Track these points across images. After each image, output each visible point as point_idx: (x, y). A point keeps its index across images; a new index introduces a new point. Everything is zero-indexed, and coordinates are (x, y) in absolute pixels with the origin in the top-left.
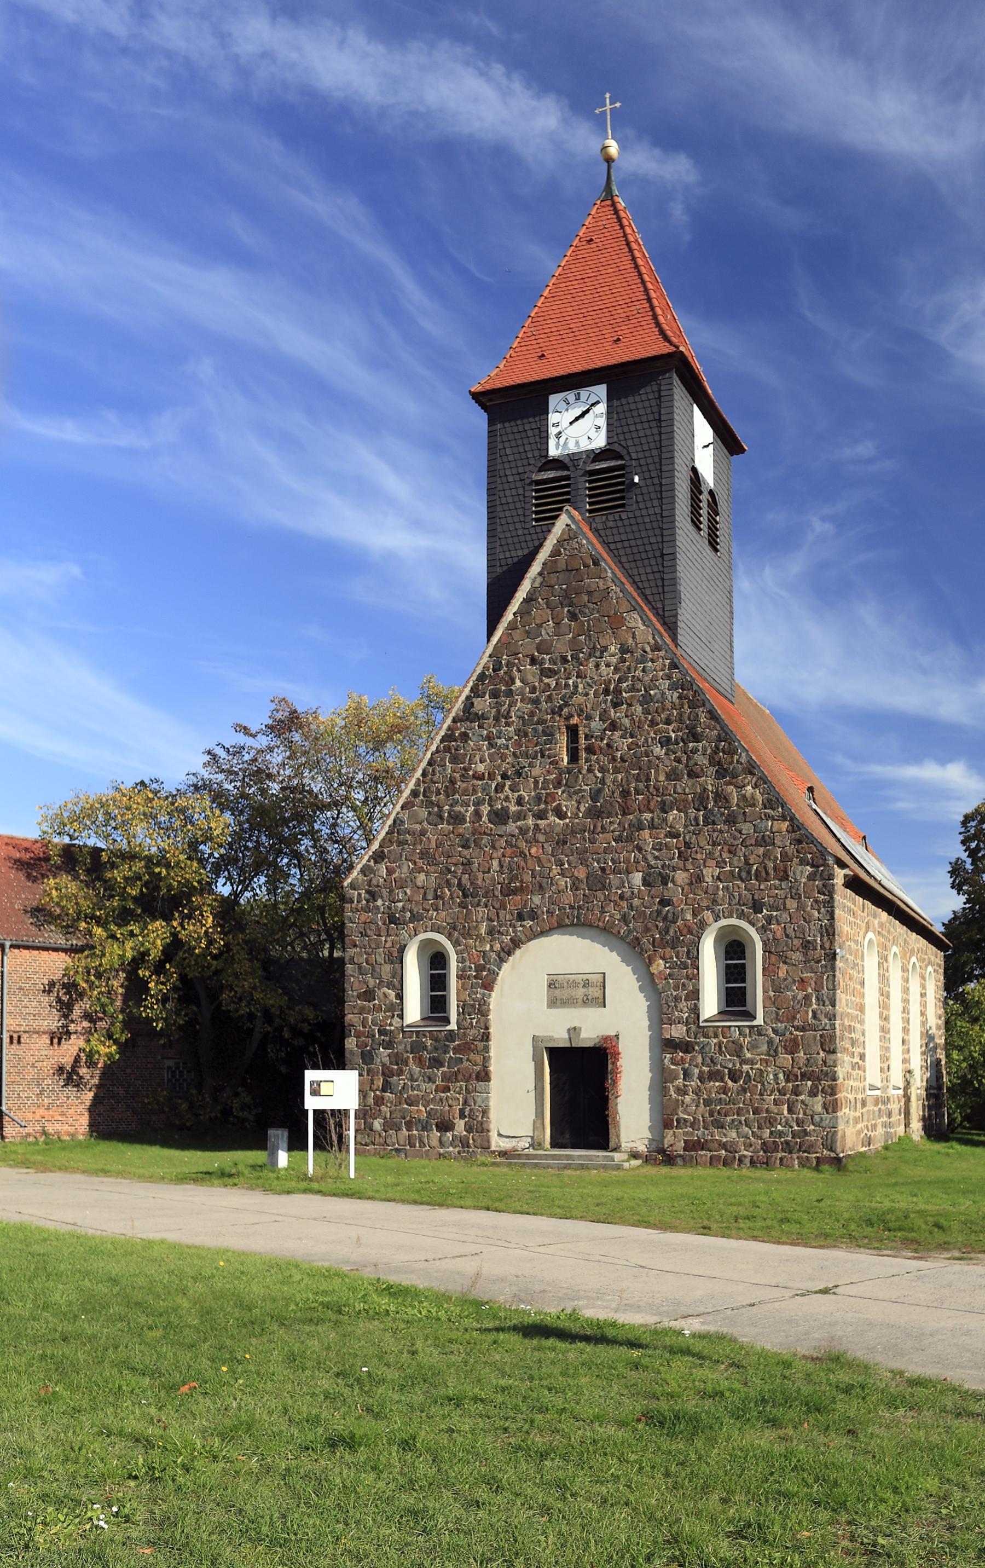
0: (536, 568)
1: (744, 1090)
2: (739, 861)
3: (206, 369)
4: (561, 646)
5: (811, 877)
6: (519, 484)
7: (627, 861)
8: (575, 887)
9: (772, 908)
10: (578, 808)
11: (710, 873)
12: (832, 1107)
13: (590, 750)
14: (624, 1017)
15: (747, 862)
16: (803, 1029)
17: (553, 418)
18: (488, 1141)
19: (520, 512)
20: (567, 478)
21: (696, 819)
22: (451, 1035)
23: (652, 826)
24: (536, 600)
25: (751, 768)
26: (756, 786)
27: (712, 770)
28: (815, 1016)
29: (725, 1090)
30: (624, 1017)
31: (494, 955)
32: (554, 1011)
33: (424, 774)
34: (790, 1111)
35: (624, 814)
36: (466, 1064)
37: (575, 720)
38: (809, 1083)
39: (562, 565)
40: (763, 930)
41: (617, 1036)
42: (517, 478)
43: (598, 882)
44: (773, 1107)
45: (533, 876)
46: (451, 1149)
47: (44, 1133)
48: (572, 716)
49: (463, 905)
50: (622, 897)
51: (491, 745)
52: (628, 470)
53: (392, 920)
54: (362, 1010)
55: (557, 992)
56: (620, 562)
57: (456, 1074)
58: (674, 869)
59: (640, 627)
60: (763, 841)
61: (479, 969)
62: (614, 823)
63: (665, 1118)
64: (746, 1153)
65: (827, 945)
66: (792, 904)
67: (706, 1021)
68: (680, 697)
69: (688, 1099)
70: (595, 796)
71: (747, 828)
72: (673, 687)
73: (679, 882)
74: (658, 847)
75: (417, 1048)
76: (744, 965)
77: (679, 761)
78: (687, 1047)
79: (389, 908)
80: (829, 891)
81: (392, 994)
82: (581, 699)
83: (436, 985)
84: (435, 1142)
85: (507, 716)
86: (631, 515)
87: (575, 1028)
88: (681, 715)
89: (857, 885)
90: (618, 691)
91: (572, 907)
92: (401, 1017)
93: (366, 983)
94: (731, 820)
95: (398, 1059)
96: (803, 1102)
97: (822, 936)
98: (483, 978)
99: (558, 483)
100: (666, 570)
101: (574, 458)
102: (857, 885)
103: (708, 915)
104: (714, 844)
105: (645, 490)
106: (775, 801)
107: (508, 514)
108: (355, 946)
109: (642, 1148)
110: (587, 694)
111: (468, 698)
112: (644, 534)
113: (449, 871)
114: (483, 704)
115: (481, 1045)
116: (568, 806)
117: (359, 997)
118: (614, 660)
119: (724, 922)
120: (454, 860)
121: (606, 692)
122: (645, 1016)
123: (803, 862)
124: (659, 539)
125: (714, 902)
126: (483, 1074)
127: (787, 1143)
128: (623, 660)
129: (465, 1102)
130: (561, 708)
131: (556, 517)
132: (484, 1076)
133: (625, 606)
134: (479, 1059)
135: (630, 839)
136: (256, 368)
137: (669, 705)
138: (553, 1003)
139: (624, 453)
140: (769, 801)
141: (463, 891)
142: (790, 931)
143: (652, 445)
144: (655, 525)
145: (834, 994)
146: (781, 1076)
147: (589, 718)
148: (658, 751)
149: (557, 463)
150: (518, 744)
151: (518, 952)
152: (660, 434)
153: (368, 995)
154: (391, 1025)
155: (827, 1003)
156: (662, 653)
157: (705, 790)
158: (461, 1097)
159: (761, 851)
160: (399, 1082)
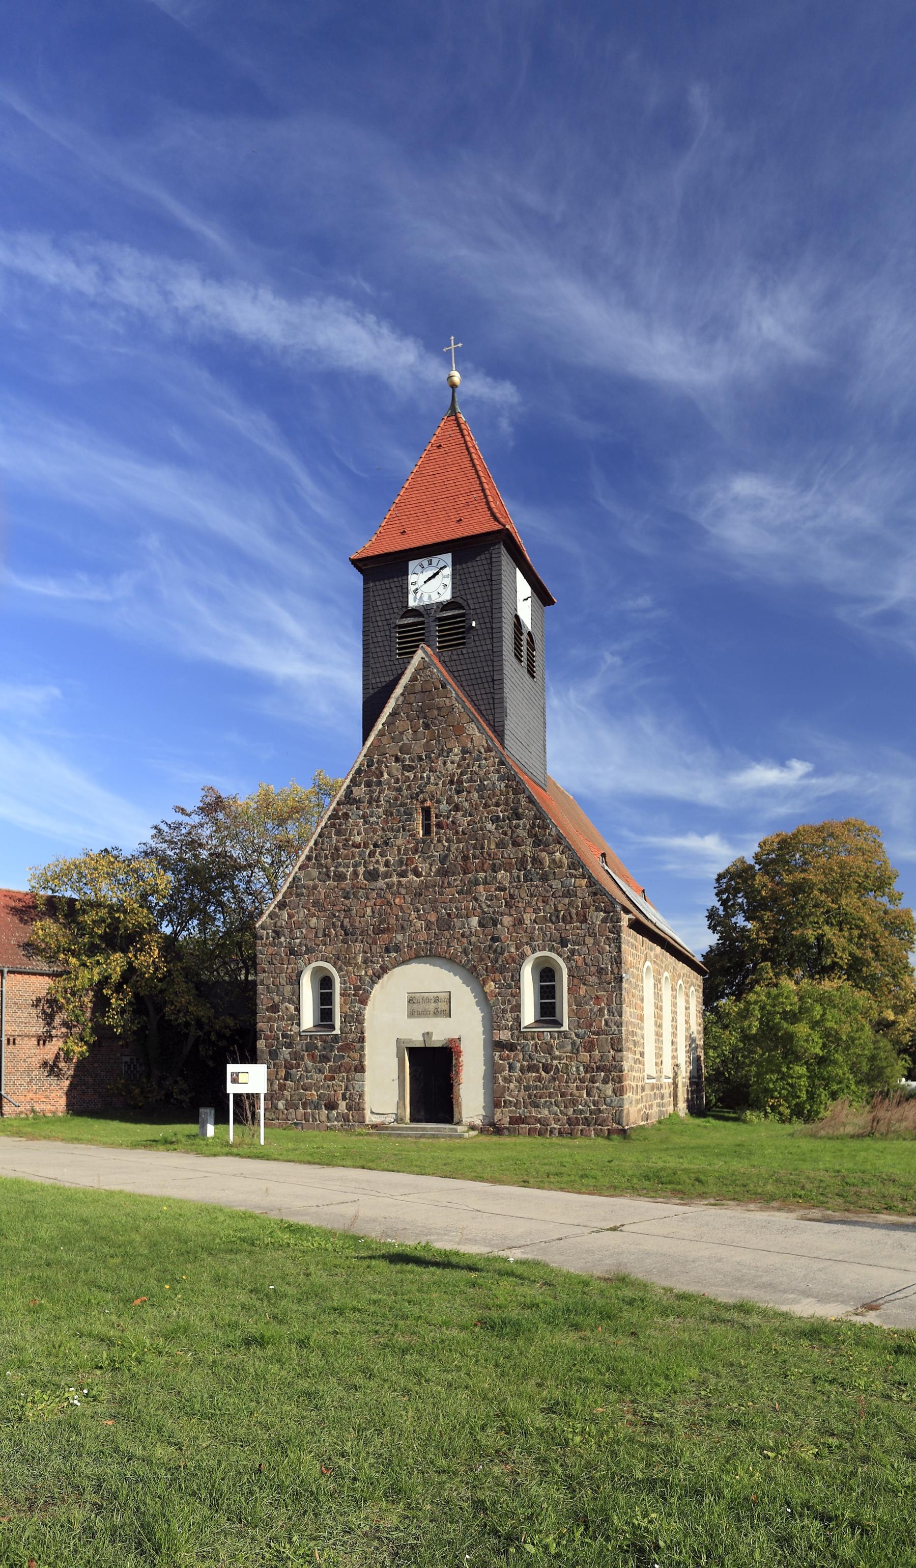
0: (399, 690)
1: (554, 1079)
2: (550, 908)
4: (418, 748)
5: (604, 921)
6: (386, 628)
7: (467, 908)
8: (428, 928)
9: (574, 943)
10: (430, 869)
11: (528, 917)
12: (619, 1092)
13: (439, 826)
14: (464, 1025)
15: (556, 910)
16: (598, 1034)
17: (412, 578)
18: (364, 1117)
19: (387, 648)
20: (422, 623)
21: (518, 877)
22: (336, 1038)
23: (486, 882)
24: (399, 714)
25: (559, 839)
26: (563, 853)
27: (531, 840)
28: (606, 1024)
29: (539, 1079)
30: (464, 1025)
31: (367, 979)
32: (413, 1020)
33: (316, 844)
34: (588, 1094)
35: (465, 873)
36: (347, 1059)
37: (428, 804)
38: (603, 1074)
39: (418, 688)
40: (568, 960)
41: (459, 1039)
42: (385, 623)
43: (445, 924)
44: (575, 1092)
45: (397, 920)
46: (336, 1123)
48: (426, 800)
49: (344, 942)
50: (463, 935)
51: (366, 822)
52: (467, 617)
53: (292, 952)
54: (270, 1019)
55: (415, 1005)
56: (462, 686)
57: (340, 1067)
58: (502, 914)
59: (477, 734)
60: (568, 894)
61: (357, 989)
62: (457, 880)
63: (495, 1100)
64: (555, 1126)
65: (616, 971)
66: (589, 941)
67: (525, 1028)
68: (506, 787)
69: (512, 1086)
70: (443, 859)
71: (556, 884)
72: (501, 779)
73: (506, 924)
74: (490, 898)
75: (310, 1047)
76: (554, 986)
77: (505, 834)
78: (511, 1047)
79: (290, 943)
80: (617, 931)
81: (292, 1007)
82: (433, 788)
83: (325, 999)
84: (324, 1118)
85: (378, 801)
86: (470, 650)
88: (507, 799)
89: (639, 926)
90: (460, 782)
91: (426, 943)
92: (299, 1024)
93: (272, 999)
94: (544, 878)
95: (297, 1056)
96: (598, 1088)
97: (612, 964)
98: (359, 995)
99: (415, 626)
100: (496, 692)
101: (428, 608)
102: (639, 926)
103: (527, 948)
104: (532, 896)
105: (480, 632)
106: (577, 864)
107: (378, 649)
108: (264, 972)
109: (478, 1122)
110: (437, 784)
111: (348, 787)
112: (479, 665)
113: (335, 916)
114: (360, 792)
115: (358, 1046)
116: (423, 867)
117: (267, 1010)
118: (457, 759)
119: (539, 954)
120: (338, 908)
121: (452, 782)
123: (598, 909)
124: (491, 669)
125: (532, 939)
127: (586, 1118)
128: (464, 759)
129: (347, 1088)
130: (417, 794)
131: (414, 652)
132: (360, 1069)
133: (465, 719)
134: (356, 1056)
135: (469, 892)
137: (498, 792)
138: (412, 1014)
139: (464, 604)
140: (573, 863)
141: (345, 931)
142: (588, 961)
143: (486, 599)
144: (488, 658)
145: (621, 1008)
146: (581, 1068)
147: (438, 802)
148: (490, 826)
149: (415, 612)
150: (386, 821)
151: (386, 976)
152: (491, 590)
153: (274, 1008)
154: (291, 1030)
155: (616, 1014)
156: (493, 754)
157: (525, 855)
158: (343, 1084)
159: (567, 901)
160: (297, 1073)
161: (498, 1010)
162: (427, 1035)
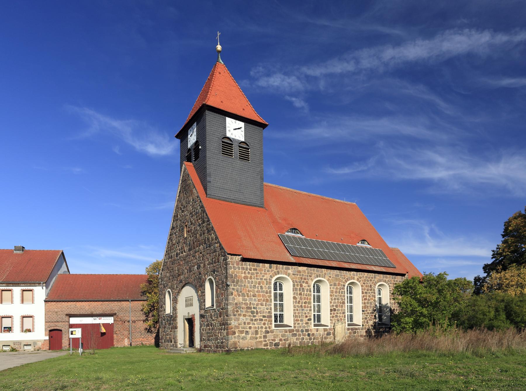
3: (381, 144)
40: (215, 279)
47: (142, 344)
94: (210, 246)
123: (222, 256)
136: (394, 140)
138: (187, 306)
148: (198, 228)
153: (162, 307)
161: (202, 301)
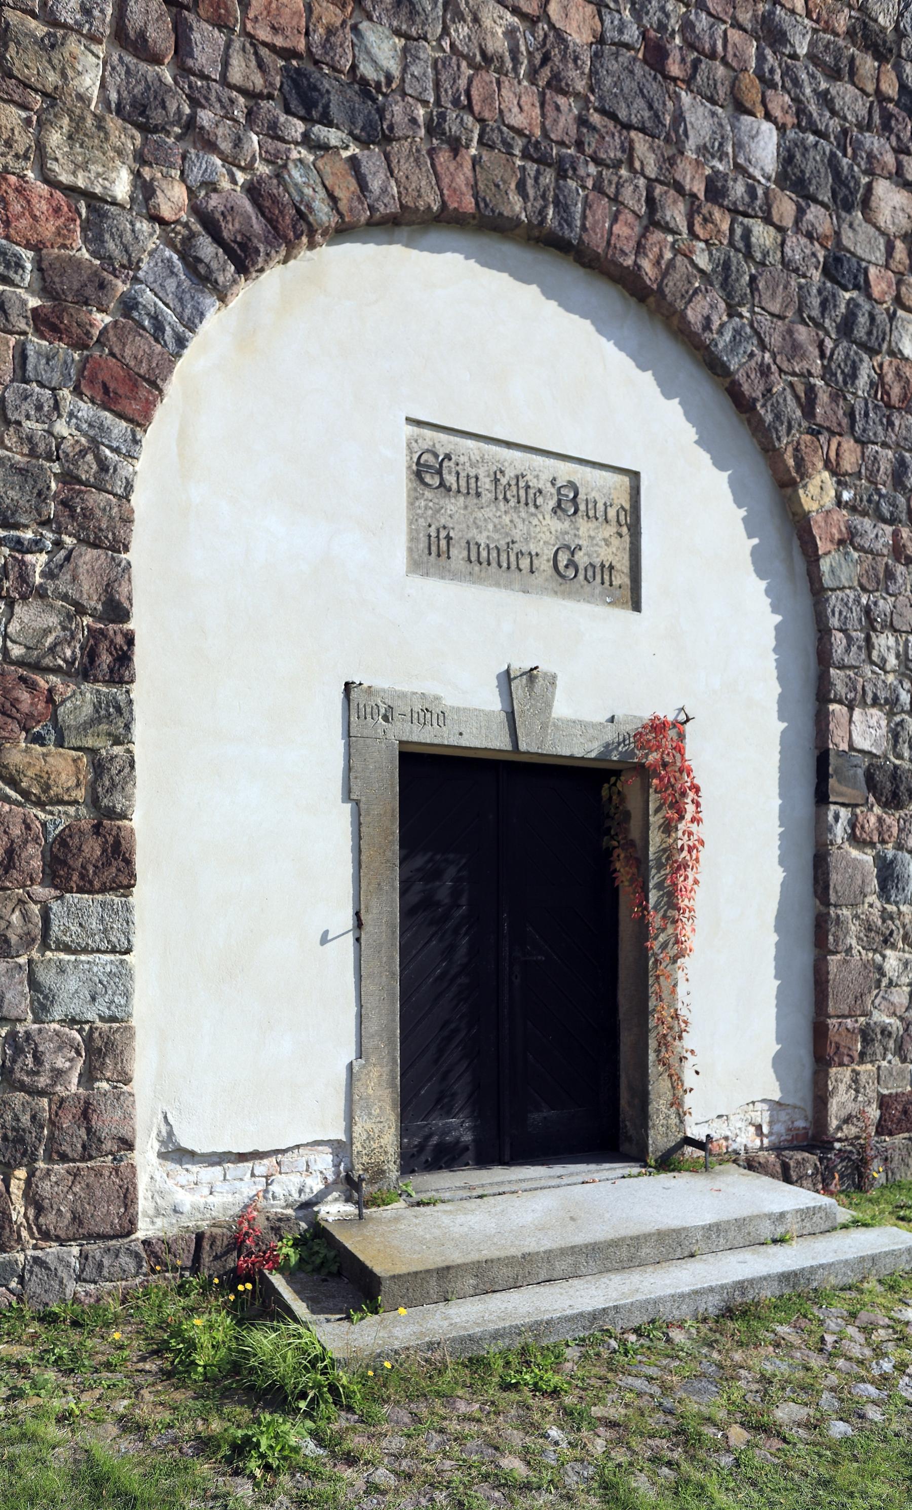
30: (687, 655)
55: (453, 506)
63: (820, 1037)
73: (884, 217)
87: (531, 674)
115: (79, 701)
122: (770, 662)
126: (93, 849)
138: (434, 550)
162: (521, 685)
